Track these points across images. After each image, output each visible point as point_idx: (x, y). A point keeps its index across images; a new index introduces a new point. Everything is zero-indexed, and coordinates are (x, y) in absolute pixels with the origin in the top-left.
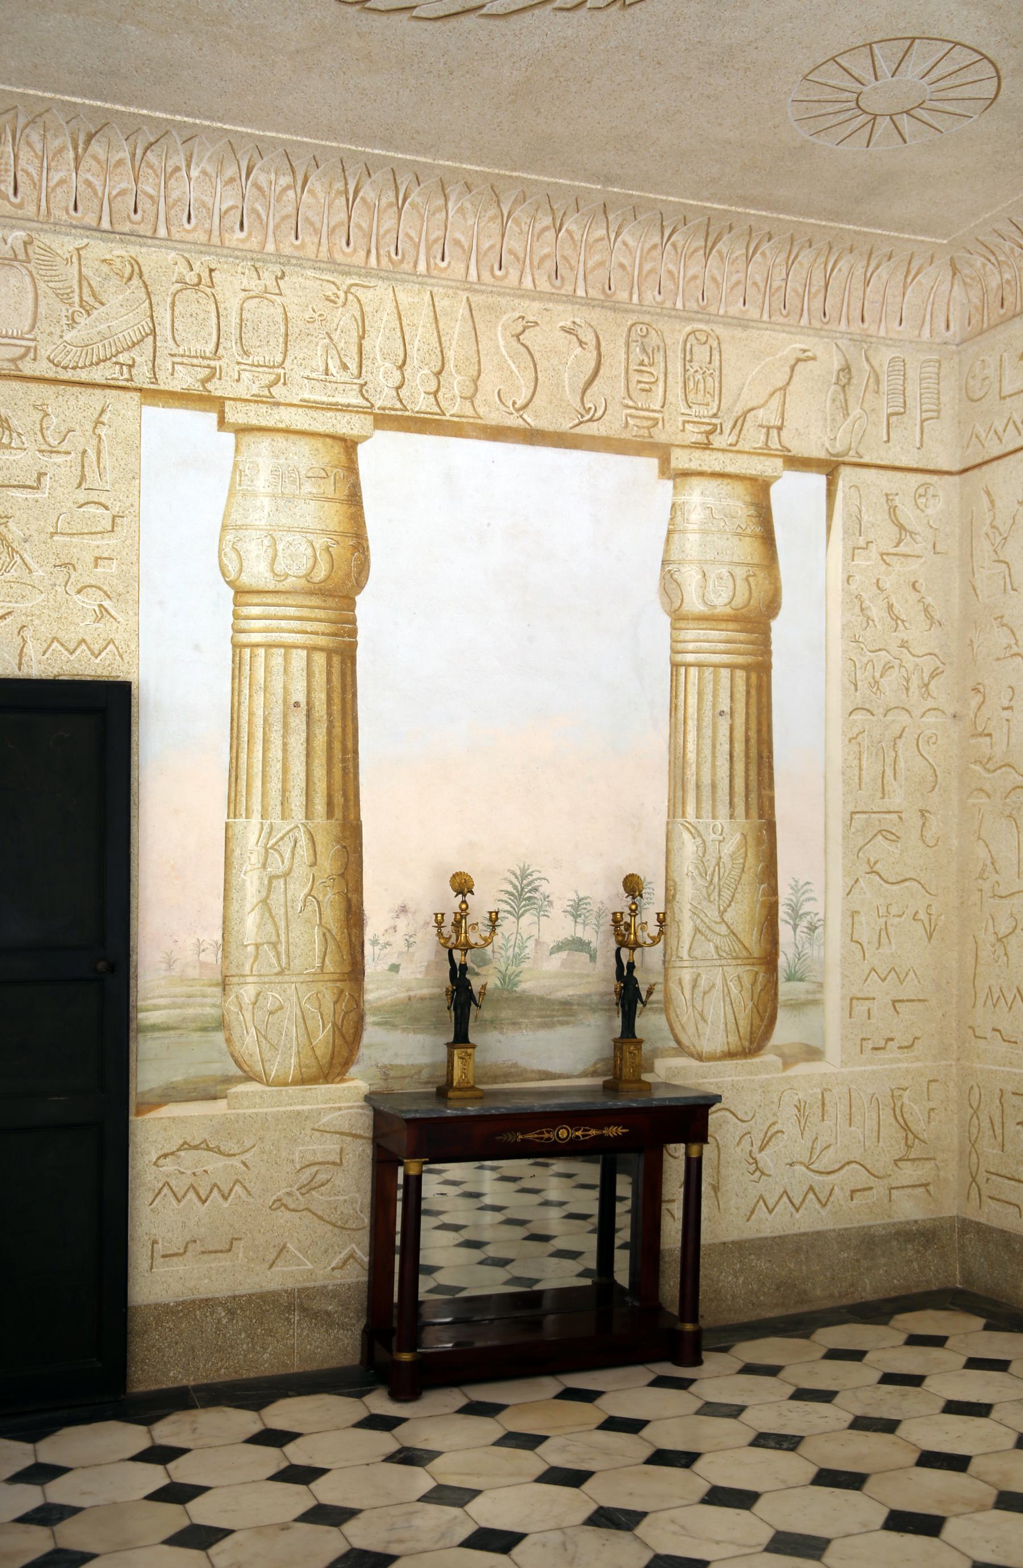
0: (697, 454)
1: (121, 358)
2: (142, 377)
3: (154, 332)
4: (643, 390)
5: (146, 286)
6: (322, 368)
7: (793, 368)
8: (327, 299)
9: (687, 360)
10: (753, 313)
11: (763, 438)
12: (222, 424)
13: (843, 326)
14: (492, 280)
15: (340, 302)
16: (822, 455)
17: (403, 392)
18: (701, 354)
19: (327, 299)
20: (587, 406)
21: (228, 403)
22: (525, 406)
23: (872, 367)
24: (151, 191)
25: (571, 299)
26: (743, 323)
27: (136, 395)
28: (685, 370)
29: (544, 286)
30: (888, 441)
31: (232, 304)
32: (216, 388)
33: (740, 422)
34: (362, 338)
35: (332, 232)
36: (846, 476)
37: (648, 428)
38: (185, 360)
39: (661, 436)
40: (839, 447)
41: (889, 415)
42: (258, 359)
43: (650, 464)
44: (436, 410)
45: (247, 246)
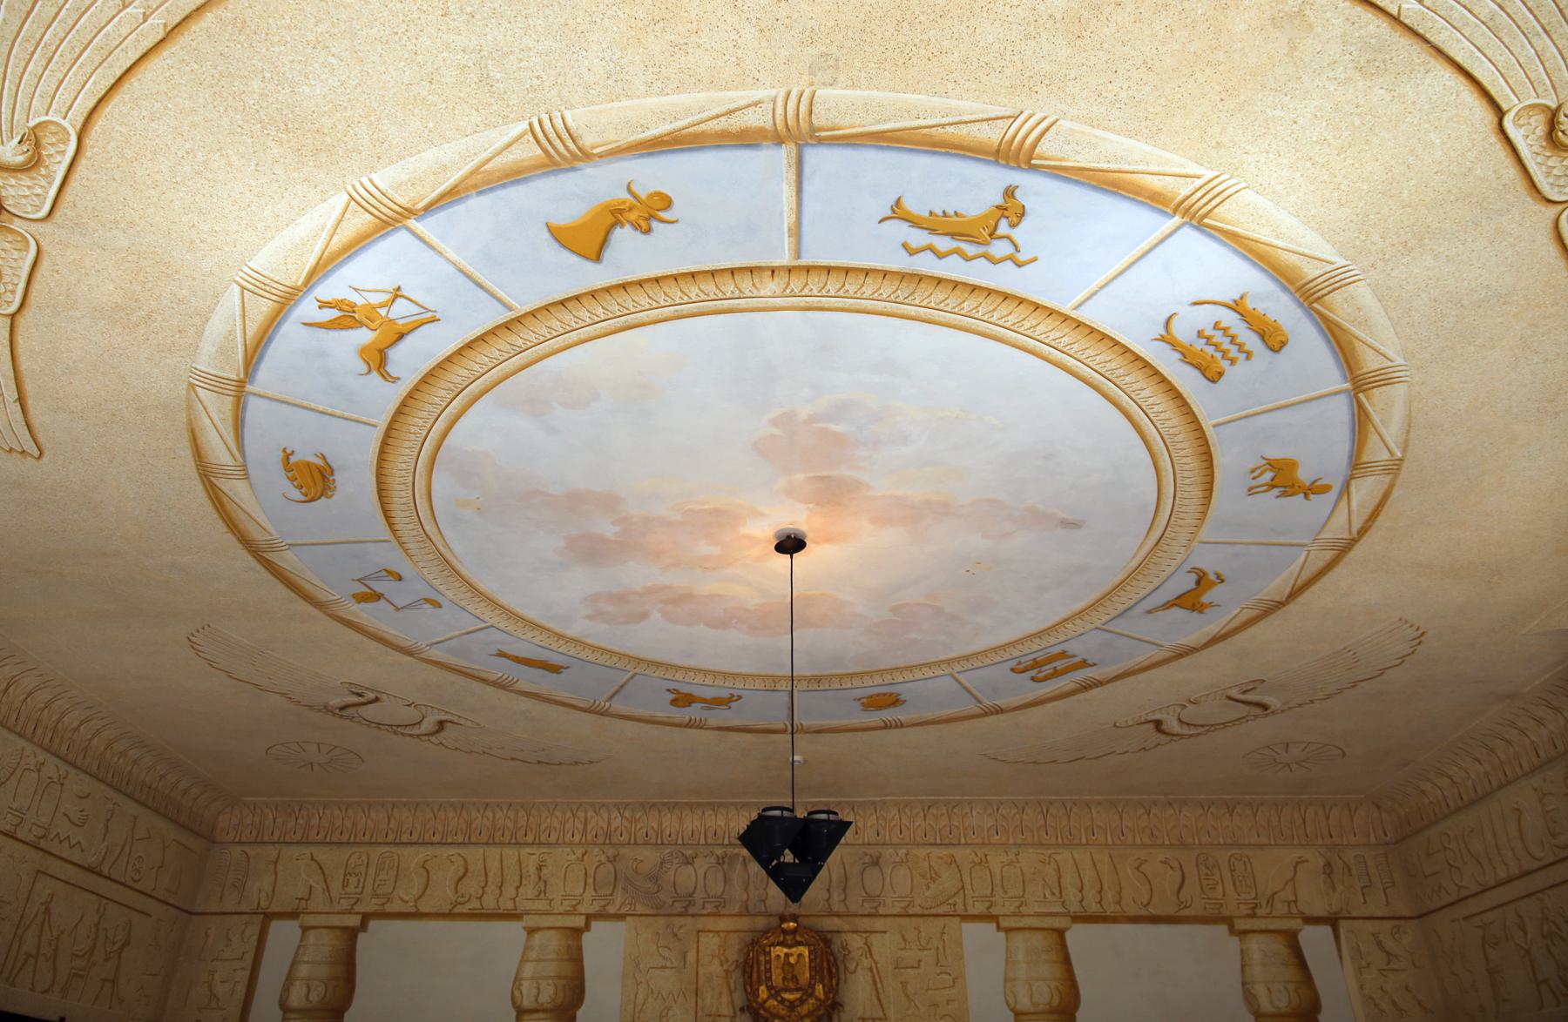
0: (1249, 920)
1: (950, 901)
2: (960, 908)
3: (963, 887)
4: (1211, 889)
5: (958, 867)
6: (1042, 896)
7: (1295, 868)
8: (1041, 862)
9: (1232, 870)
10: (1265, 841)
11: (1286, 908)
12: (999, 928)
13: (1320, 842)
14: (1119, 842)
15: (1047, 862)
16: (1325, 914)
17: (1084, 903)
18: (1239, 866)
19: (1041, 862)
20: (1182, 900)
21: (1001, 919)
22: (1148, 904)
23: (1343, 861)
24: (957, 824)
25: (1163, 845)
26: (1260, 846)
27: (958, 919)
28: (1232, 876)
29: (1147, 841)
30: (1365, 902)
31: (997, 870)
32: (994, 911)
33: (1271, 900)
34: (1059, 878)
35: (1039, 829)
36: (1344, 926)
37: (1218, 909)
38: (980, 899)
39: (1226, 913)
40: (1335, 908)
41: (1362, 888)
42: (1010, 895)
43: (1224, 928)
44: (1102, 910)
45: (1001, 842)
